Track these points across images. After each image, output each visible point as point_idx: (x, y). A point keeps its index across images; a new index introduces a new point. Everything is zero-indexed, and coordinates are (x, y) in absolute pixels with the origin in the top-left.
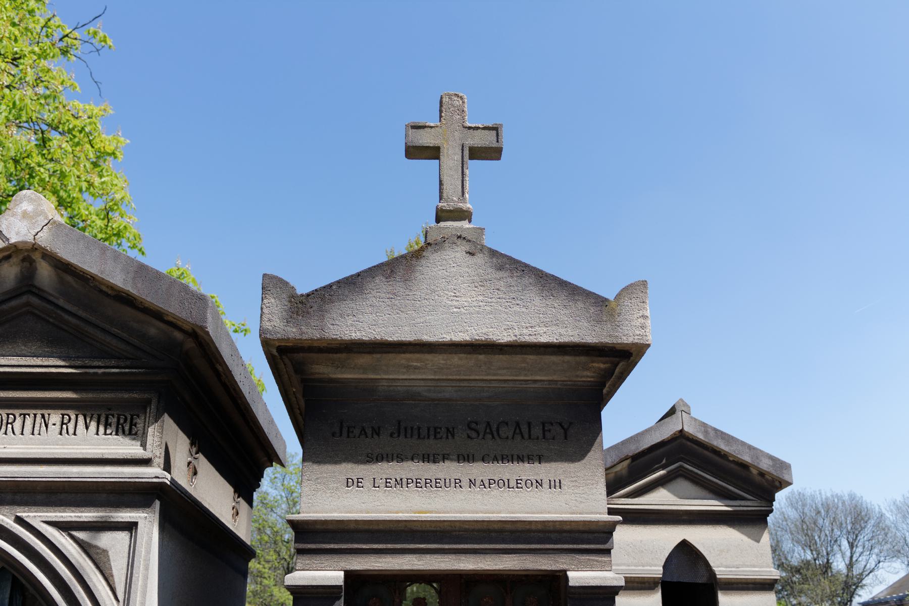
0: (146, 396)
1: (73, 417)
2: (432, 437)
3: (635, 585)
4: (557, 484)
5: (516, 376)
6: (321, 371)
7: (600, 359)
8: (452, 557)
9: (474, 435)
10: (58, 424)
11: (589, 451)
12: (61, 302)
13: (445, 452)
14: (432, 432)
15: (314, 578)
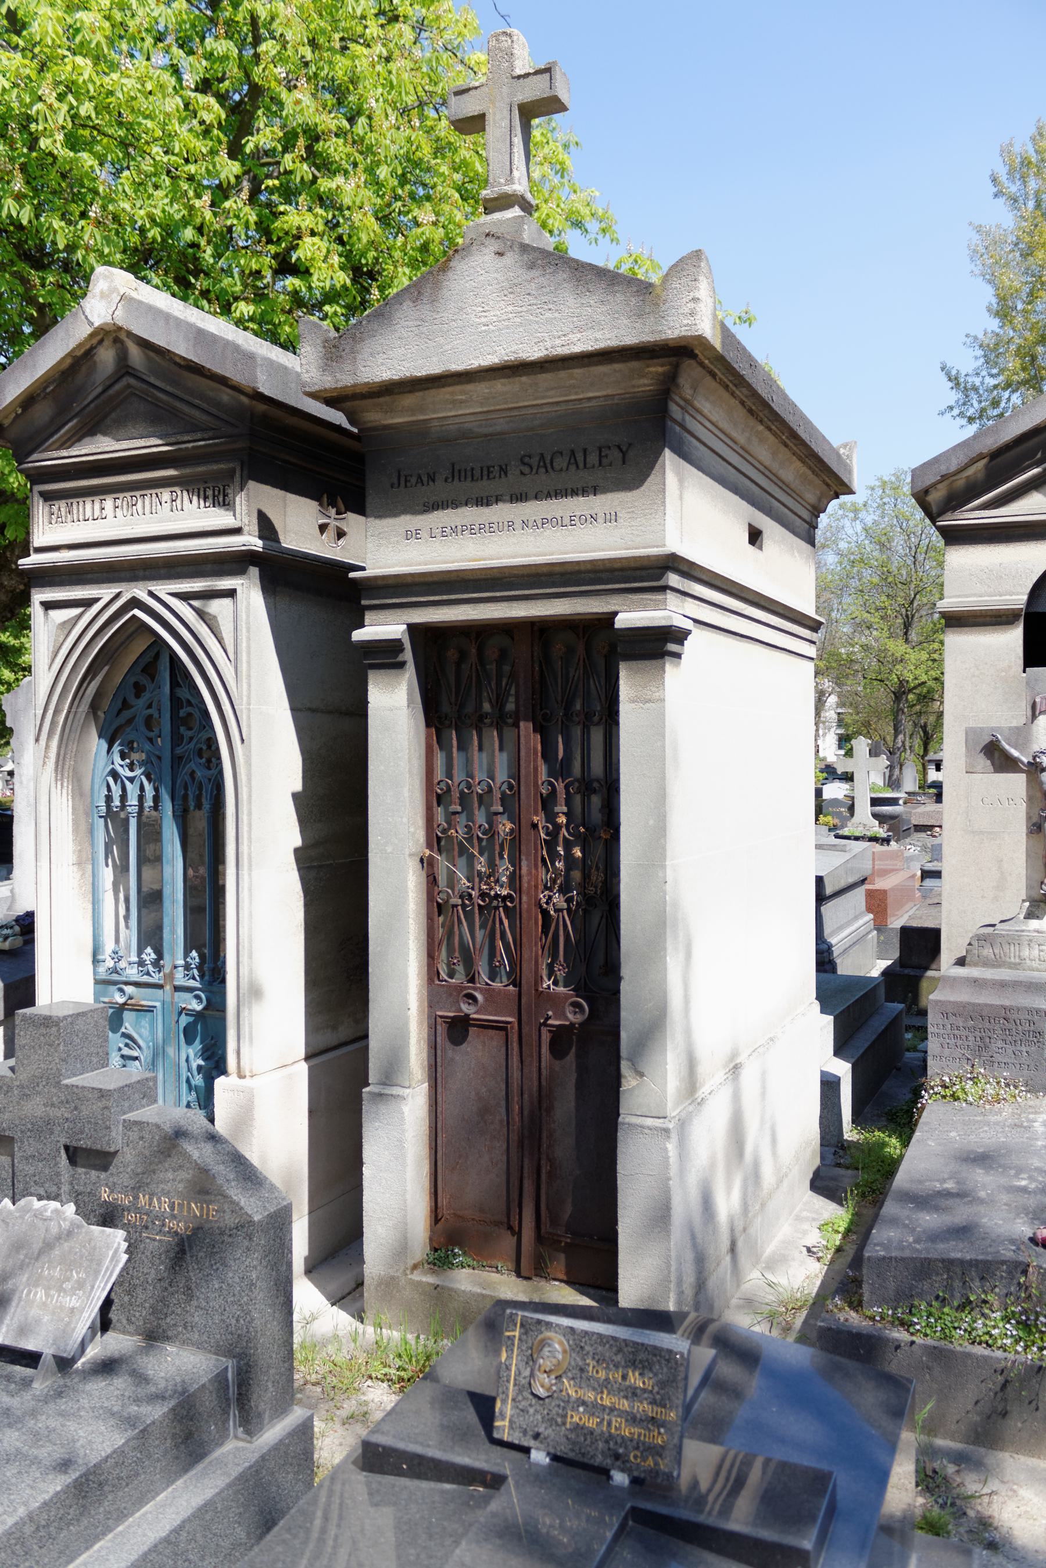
0: (231, 465)
1: (179, 493)
2: (485, 477)
3: (988, 619)
4: (613, 518)
5: (566, 395)
6: (372, 418)
7: (655, 361)
8: (504, 604)
9: (527, 470)
10: (169, 501)
11: (648, 476)
12: (152, 380)
13: (498, 493)
14: (485, 473)
15: (377, 633)
